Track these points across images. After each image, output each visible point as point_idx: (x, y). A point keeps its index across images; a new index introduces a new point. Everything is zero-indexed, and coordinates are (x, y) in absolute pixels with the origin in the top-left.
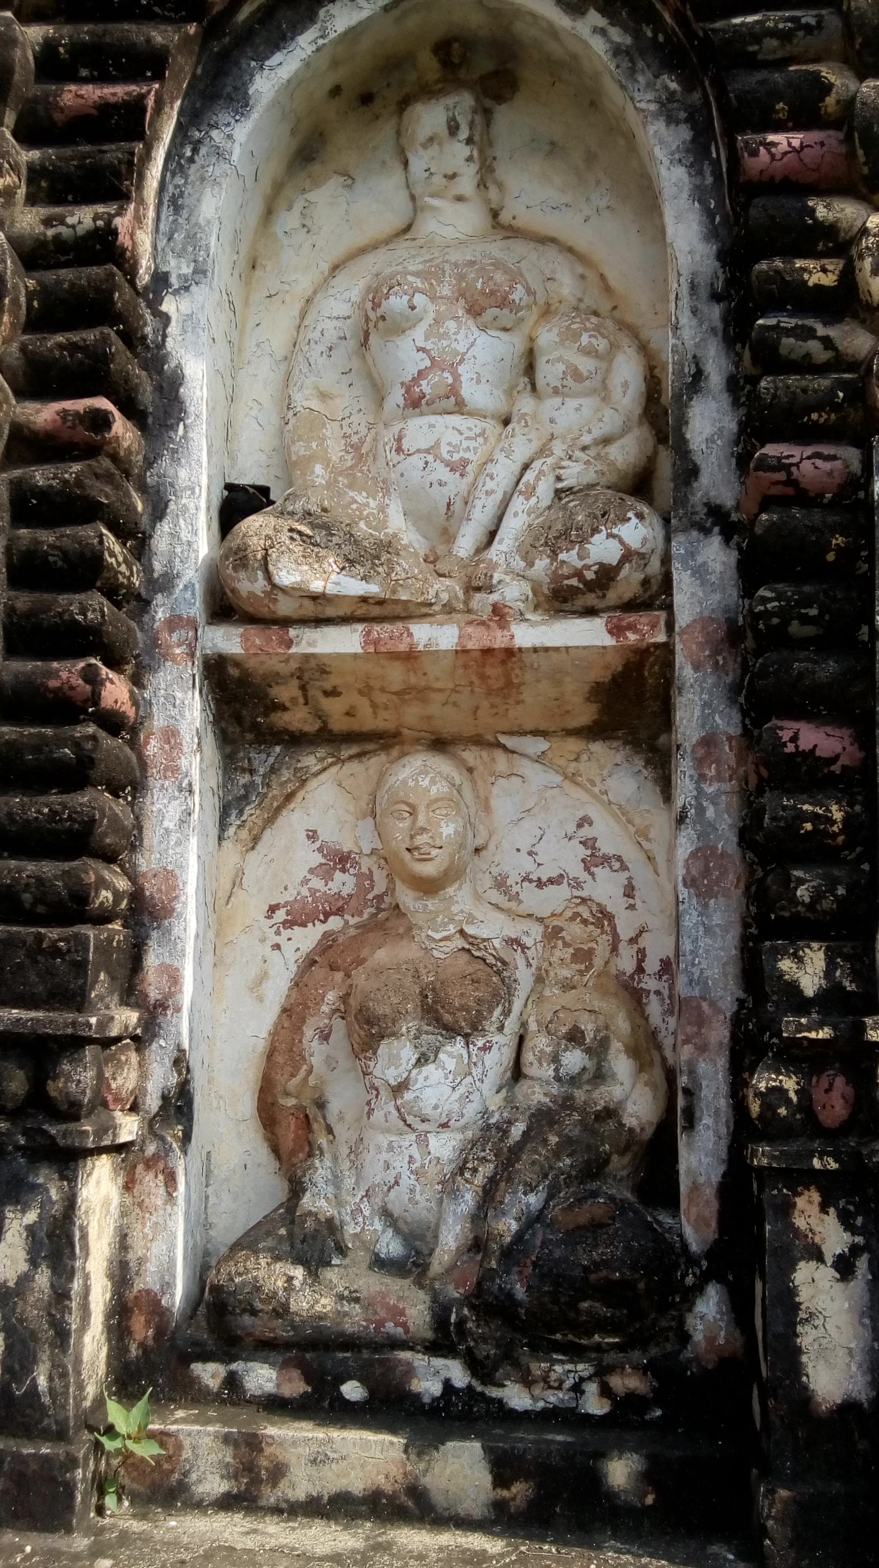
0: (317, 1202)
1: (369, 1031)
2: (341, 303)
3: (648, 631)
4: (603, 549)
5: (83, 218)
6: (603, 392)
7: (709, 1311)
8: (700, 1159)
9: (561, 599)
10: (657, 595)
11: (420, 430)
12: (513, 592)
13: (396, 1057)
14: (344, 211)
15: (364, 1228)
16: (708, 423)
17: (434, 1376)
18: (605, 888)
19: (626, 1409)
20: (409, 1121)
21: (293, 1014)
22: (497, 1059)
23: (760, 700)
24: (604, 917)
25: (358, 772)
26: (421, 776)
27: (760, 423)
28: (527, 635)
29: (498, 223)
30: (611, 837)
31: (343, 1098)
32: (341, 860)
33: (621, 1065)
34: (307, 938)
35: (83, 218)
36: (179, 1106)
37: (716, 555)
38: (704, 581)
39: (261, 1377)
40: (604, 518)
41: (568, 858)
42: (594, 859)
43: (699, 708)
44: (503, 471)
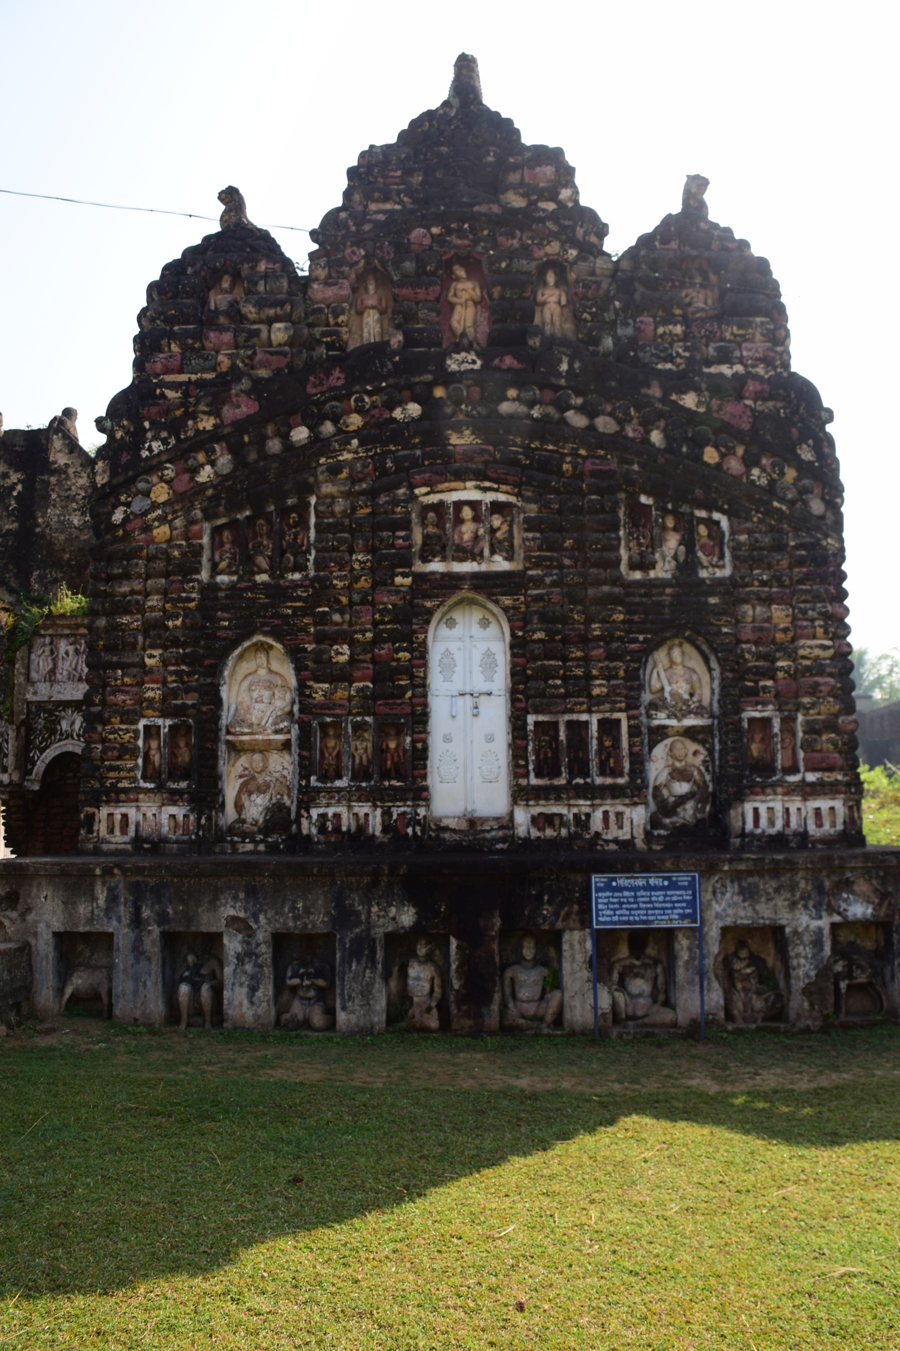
0: (243, 816)
1: (250, 793)
2: (246, 684)
3: (287, 736)
4: (282, 726)
5: (209, 680)
6: (284, 699)
7: (294, 827)
8: (294, 808)
9: (277, 732)
10: (289, 732)
11: (258, 706)
12: (269, 731)
13: (254, 797)
14: (245, 667)
15: (249, 820)
16: (296, 708)
17: (260, 837)
18: (285, 773)
19: (283, 840)
20: (256, 805)
21: (240, 791)
22: (268, 797)
23: (301, 747)
24: (285, 777)
25: (248, 755)
26: (257, 757)
27: (301, 711)
28: (273, 737)
29: (270, 671)
30: (286, 765)
31: (247, 804)
32: (246, 769)
33: (286, 797)
34: (241, 780)
35: (209, 680)
36: (223, 804)
37: (296, 726)
38: (295, 730)
39: (236, 839)
40: (282, 721)
41: (280, 768)
42: (284, 768)
43: (294, 748)
44: (269, 713)
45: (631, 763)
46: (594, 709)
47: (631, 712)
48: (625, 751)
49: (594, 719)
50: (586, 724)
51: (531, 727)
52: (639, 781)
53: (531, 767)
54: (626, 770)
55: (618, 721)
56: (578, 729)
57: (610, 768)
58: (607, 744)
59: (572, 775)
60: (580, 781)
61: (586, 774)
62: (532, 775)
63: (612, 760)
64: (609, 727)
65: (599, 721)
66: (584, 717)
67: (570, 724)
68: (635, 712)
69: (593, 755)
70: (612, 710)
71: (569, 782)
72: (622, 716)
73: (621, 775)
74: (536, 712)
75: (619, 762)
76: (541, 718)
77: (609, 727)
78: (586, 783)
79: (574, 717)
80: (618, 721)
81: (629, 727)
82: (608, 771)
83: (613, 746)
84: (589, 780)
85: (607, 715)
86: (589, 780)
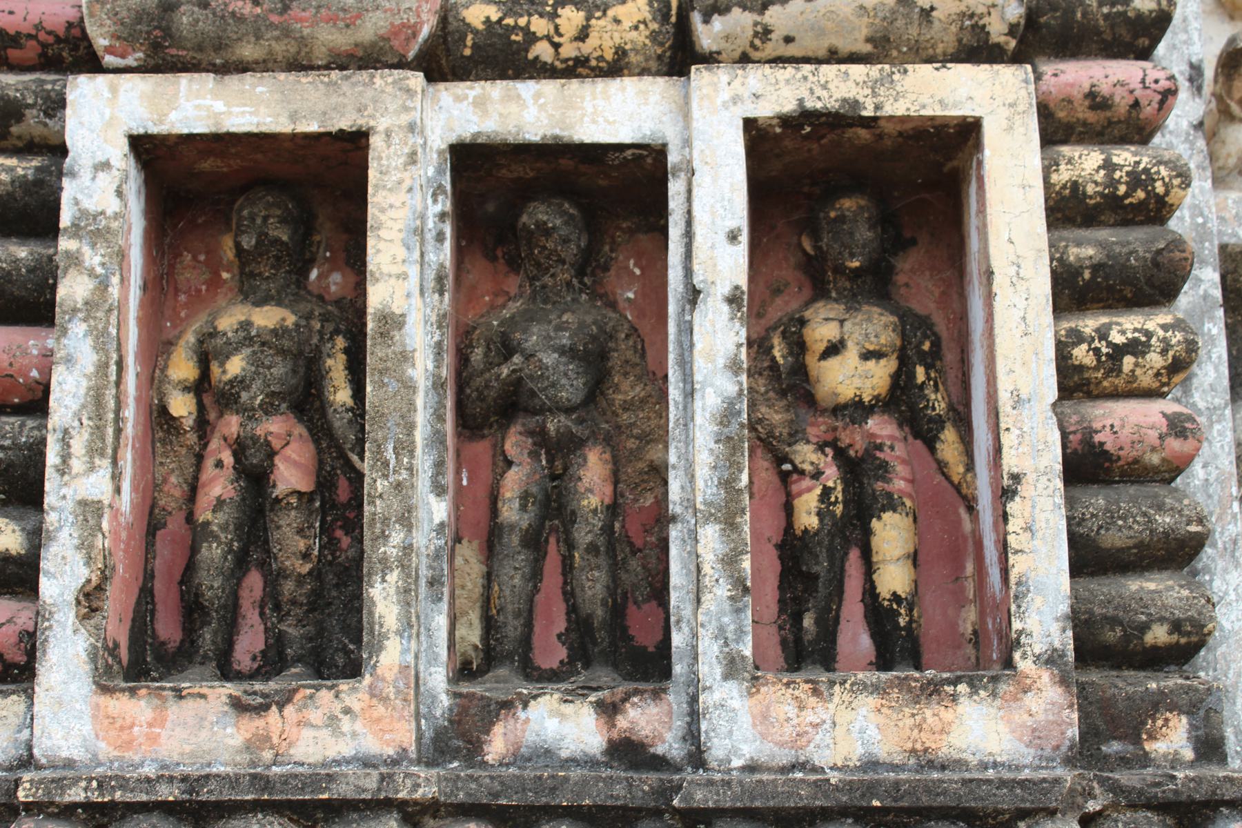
45: (1088, 558)
46: (708, 34)
47: (1077, 75)
48: (1027, 431)
49: (707, 132)
50: (628, 191)
51: (100, 187)
52: (1173, 739)
53: (62, 576)
54: (1045, 603)
55: (950, 147)
56: (563, 221)
57: (879, 615)
58: (850, 376)
59: (497, 657)
60: (561, 725)
61: (625, 646)
62: (67, 656)
63: (891, 535)
64: (863, 205)
65: (756, 135)
66: (613, 113)
67: (488, 183)
68: (1114, 75)
69: (699, 451)
70: (882, 49)
71: (457, 738)
72: (997, 101)
73: (990, 657)
74: (163, 55)
75: (960, 543)
76: (198, 106)
77: (863, 205)
78: (628, 752)
79: (525, 111)
80: (950, 147)
81: (1066, 209)
82: (855, 638)
83: (900, 399)
84: (650, 719)
85: (837, 87)
86: (650, 719)
